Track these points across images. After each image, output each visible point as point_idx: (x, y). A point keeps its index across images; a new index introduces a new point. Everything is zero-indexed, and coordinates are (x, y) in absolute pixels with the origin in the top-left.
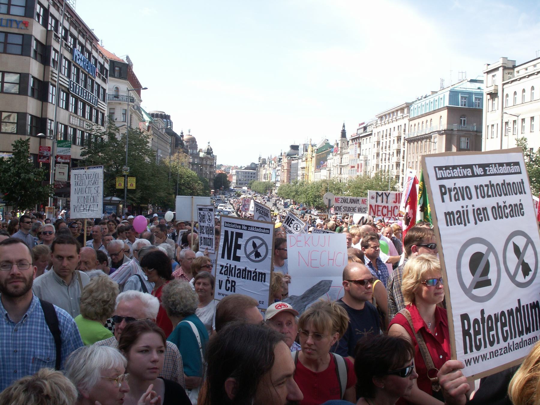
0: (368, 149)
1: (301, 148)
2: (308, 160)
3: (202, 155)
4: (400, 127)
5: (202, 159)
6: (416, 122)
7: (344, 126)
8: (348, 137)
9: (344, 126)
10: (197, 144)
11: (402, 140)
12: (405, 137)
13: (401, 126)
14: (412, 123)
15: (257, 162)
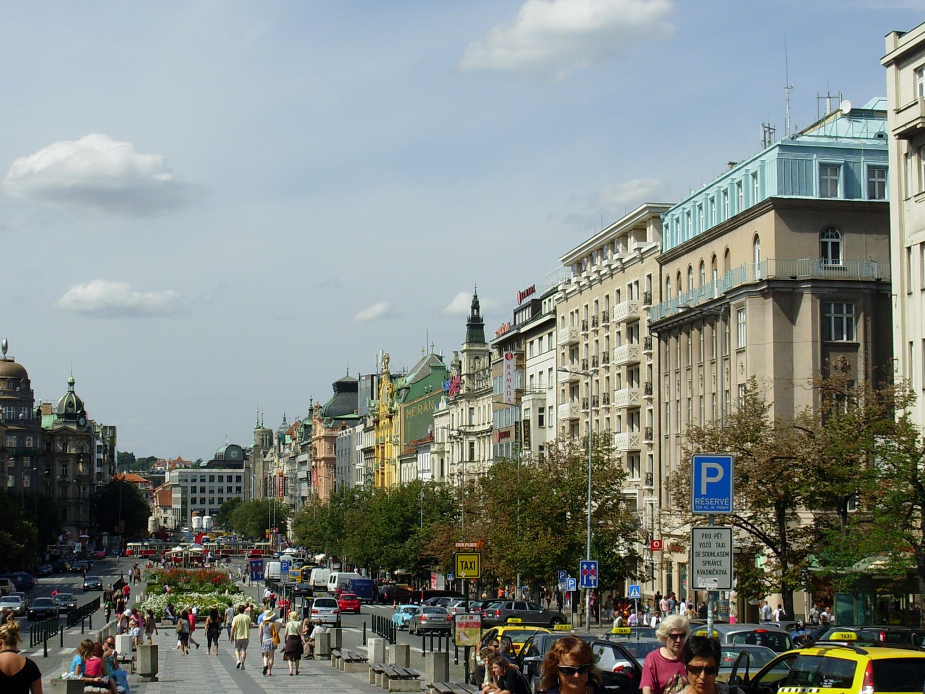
0: (546, 372)
1: (364, 386)
2: (381, 423)
3: (47, 422)
4: (634, 287)
5: (49, 436)
6: (681, 264)
7: (476, 306)
8: (491, 334)
9: (476, 306)
10: (32, 387)
11: (644, 332)
12: (649, 321)
13: (637, 283)
14: (670, 269)
15: (248, 442)
